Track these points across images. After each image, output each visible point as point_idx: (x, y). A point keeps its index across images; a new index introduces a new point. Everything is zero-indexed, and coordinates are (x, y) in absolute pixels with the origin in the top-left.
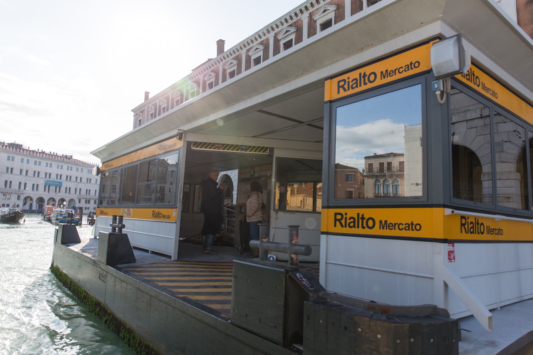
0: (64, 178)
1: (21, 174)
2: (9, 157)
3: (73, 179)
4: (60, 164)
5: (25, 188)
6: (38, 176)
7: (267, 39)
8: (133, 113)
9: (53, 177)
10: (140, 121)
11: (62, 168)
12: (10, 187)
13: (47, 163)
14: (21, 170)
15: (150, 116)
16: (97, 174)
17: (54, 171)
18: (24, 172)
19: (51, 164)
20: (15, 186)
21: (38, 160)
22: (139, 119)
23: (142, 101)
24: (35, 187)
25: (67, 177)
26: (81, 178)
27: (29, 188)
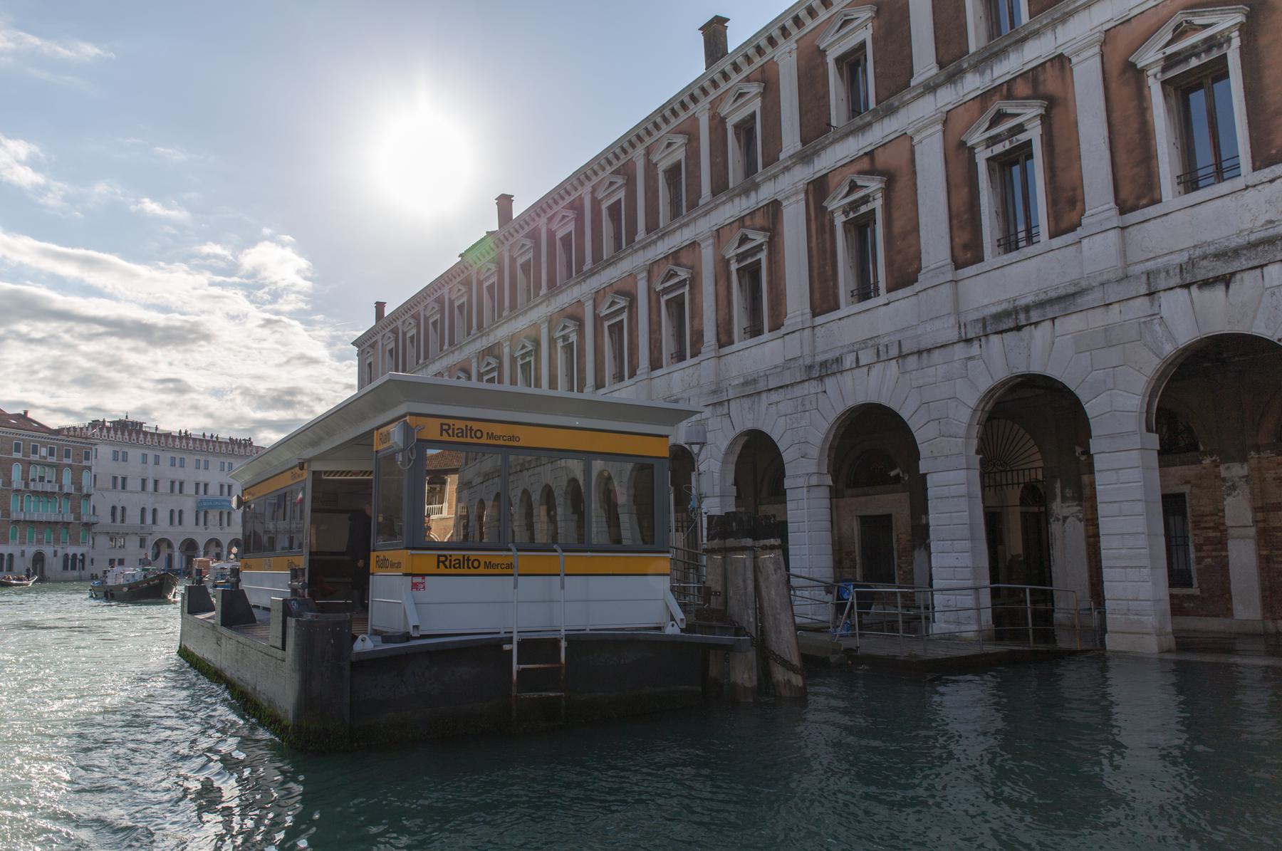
1: (143, 488)
2: (115, 453)
4: (227, 461)
5: (154, 522)
6: (181, 492)
7: (581, 198)
10: (370, 365)
12: (123, 521)
14: (144, 481)
15: (387, 354)
16: (238, 507)
19: (207, 462)
20: (133, 517)
21: (178, 456)
23: (369, 321)
24: (176, 517)
27: (163, 516)
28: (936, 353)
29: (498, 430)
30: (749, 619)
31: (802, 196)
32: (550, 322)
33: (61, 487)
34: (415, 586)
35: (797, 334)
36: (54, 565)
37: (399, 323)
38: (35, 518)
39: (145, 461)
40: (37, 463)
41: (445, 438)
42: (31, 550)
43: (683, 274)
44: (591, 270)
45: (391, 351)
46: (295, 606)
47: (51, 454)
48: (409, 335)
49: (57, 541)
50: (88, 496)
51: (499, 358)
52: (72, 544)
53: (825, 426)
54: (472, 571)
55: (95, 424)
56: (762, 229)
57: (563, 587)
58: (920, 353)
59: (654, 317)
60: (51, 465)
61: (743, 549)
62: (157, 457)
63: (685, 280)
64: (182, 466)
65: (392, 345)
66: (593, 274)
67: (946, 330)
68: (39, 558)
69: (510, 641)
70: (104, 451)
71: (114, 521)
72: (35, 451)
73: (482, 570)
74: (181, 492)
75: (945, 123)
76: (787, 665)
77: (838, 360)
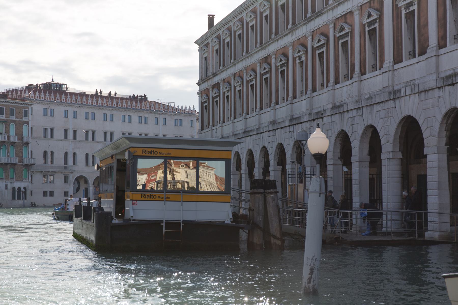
1: (66, 137)
2: (45, 110)
4: (127, 114)
5: (74, 163)
6: (93, 139)
8: (197, 47)
10: (206, 58)
11: (130, 121)
12: (52, 162)
13: (105, 115)
14: (66, 131)
15: (215, 52)
16: (98, 169)
18: (71, 135)
19: (112, 116)
20: (59, 159)
21: (90, 111)
22: (204, 57)
23: (205, 29)
27: (81, 158)
28: (430, 92)
30: (259, 219)
33: (9, 138)
34: (133, 204)
35: (387, 73)
37: (221, 32)
39: (66, 116)
41: (144, 154)
43: (347, 30)
44: (310, 17)
45: (217, 50)
46: (97, 209)
48: (226, 41)
49: (7, 178)
50: (27, 144)
51: (270, 64)
52: (17, 180)
53: (395, 126)
54: (153, 199)
55: (30, 88)
56: (377, 10)
57: (182, 205)
58: (425, 91)
59: (337, 52)
61: (259, 193)
62: (75, 112)
63: (348, 33)
65: (217, 47)
66: (312, 20)
67: (431, 82)
69: (163, 223)
70: (38, 108)
71: (45, 162)
74: (93, 139)
76: (275, 237)
77: (399, 91)
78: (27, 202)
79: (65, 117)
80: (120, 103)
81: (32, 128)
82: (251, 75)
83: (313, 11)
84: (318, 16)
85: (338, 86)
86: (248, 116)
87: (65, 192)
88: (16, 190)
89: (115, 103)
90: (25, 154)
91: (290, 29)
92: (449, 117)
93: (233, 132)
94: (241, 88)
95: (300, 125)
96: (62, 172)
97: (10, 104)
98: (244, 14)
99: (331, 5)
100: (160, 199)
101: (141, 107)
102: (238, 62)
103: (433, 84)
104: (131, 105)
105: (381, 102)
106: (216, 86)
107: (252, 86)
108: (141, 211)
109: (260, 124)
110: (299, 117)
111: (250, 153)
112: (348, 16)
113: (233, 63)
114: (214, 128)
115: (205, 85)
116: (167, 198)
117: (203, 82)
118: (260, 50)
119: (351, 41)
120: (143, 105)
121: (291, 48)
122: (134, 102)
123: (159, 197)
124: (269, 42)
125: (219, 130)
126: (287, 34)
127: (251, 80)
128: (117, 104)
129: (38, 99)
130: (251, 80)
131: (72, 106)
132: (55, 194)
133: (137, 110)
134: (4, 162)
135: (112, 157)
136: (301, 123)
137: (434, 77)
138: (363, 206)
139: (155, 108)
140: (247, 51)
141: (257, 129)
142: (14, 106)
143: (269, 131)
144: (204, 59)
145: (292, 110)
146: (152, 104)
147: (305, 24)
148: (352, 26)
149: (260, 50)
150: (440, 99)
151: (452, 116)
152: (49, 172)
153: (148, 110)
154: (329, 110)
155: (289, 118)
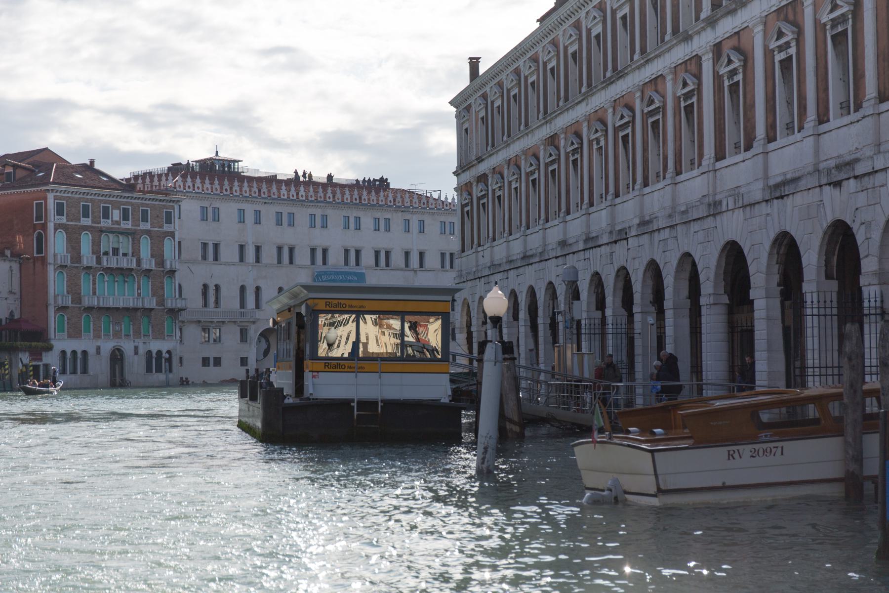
0: (368, 259)
1: (242, 259)
2: (204, 210)
3: (397, 259)
4: (353, 214)
5: (258, 306)
6: (291, 261)
8: (453, 110)
9: (336, 259)
10: (466, 130)
11: (358, 227)
14: (242, 247)
15: (480, 121)
17: (335, 238)
19: (325, 218)
20: (230, 300)
21: (285, 210)
22: (465, 128)
23: (464, 82)
25: (377, 253)
26: (421, 255)
28: (757, 206)
29: (354, 303)
31: (711, 55)
32: (589, 121)
33: (139, 262)
34: (314, 377)
36: (135, 365)
37: (487, 89)
38: (111, 304)
39: (242, 220)
40: (110, 231)
41: (328, 308)
42: (107, 346)
43: (657, 104)
44: (610, 78)
45: (482, 118)
46: (264, 385)
47: (125, 217)
48: (496, 105)
49: (137, 334)
50: (172, 272)
52: (155, 338)
53: (716, 255)
55: (176, 169)
56: (695, 76)
60: (125, 233)
62: (258, 213)
63: (659, 108)
64: (291, 224)
65: (482, 114)
66: (612, 83)
67: (757, 192)
68: (117, 357)
70: (190, 208)
71: (206, 305)
72: (106, 216)
73: (346, 370)
74: (291, 261)
75: (765, 24)
78: (174, 377)
79: (240, 222)
80: (338, 195)
81: (180, 243)
82: (531, 165)
83: (615, 68)
84: (620, 77)
85: (647, 190)
86: (528, 232)
87: (242, 359)
88: (154, 355)
89: (329, 194)
90: (169, 290)
91: (584, 94)
92: (780, 245)
93: (508, 257)
94: (518, 185)
95: (599, 249)
96: (235, 322)
97: (139, 201)
98: (521, 63)
99: (638, 61)
100: (351, 369)
101: (378, 200)
102: (514, 142)
103: (758, 196)
104: (360, 198)
105: (699, 219)
106: (482, 178)
107: (534, 181)
108: (325, 387)
109: (545, 245)
110: (597, 237)
111: (532, 292)
112: (659, 81)
113: (506, 142)
114: (480, 249)
115: (467, 176)
116: (360, 368)
117: (463, 172)
118: (543, 124)
119: (663, 121)
120: (382, 197)
121: (585, 124)
122: (365, 193)
123: (349, 367)
124: (555, 112)
125: (487, 253)
126: (580, 102)
127: (532, 173)
128: (334, 197)
129: (191, 190)
130: (532, 173)
131: (253, 202)
132: (223, 362)
133: (371, 206)
134: (131, 305)
135: (289, 310)
136: (599, 246)
137: (760, 185)
138: (655, 377)
139: (403, 201)
140: (526, 125)
141: (541, 253)
142: (147, 205)
143: (556, 257)
144: (464, 131)
145: (588, 225)
146: (399, 196)
147: (603, 88)
148: (663, 96)
149: (543, 124)
150: (768, 218)
151: (785, 242)
152: (212, 322)
153: (390, 206)
154: (635, 226)
155: (584, 238)
